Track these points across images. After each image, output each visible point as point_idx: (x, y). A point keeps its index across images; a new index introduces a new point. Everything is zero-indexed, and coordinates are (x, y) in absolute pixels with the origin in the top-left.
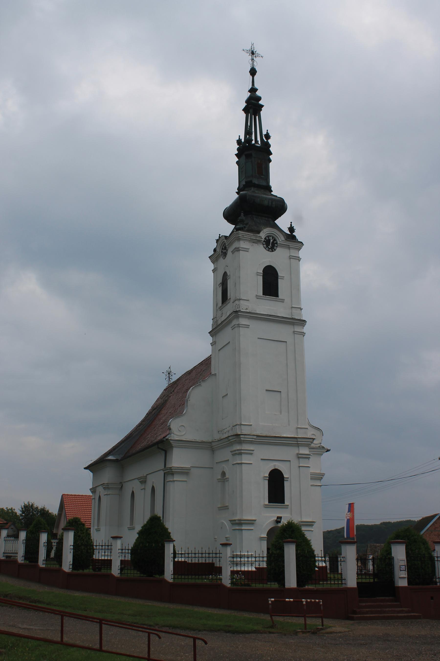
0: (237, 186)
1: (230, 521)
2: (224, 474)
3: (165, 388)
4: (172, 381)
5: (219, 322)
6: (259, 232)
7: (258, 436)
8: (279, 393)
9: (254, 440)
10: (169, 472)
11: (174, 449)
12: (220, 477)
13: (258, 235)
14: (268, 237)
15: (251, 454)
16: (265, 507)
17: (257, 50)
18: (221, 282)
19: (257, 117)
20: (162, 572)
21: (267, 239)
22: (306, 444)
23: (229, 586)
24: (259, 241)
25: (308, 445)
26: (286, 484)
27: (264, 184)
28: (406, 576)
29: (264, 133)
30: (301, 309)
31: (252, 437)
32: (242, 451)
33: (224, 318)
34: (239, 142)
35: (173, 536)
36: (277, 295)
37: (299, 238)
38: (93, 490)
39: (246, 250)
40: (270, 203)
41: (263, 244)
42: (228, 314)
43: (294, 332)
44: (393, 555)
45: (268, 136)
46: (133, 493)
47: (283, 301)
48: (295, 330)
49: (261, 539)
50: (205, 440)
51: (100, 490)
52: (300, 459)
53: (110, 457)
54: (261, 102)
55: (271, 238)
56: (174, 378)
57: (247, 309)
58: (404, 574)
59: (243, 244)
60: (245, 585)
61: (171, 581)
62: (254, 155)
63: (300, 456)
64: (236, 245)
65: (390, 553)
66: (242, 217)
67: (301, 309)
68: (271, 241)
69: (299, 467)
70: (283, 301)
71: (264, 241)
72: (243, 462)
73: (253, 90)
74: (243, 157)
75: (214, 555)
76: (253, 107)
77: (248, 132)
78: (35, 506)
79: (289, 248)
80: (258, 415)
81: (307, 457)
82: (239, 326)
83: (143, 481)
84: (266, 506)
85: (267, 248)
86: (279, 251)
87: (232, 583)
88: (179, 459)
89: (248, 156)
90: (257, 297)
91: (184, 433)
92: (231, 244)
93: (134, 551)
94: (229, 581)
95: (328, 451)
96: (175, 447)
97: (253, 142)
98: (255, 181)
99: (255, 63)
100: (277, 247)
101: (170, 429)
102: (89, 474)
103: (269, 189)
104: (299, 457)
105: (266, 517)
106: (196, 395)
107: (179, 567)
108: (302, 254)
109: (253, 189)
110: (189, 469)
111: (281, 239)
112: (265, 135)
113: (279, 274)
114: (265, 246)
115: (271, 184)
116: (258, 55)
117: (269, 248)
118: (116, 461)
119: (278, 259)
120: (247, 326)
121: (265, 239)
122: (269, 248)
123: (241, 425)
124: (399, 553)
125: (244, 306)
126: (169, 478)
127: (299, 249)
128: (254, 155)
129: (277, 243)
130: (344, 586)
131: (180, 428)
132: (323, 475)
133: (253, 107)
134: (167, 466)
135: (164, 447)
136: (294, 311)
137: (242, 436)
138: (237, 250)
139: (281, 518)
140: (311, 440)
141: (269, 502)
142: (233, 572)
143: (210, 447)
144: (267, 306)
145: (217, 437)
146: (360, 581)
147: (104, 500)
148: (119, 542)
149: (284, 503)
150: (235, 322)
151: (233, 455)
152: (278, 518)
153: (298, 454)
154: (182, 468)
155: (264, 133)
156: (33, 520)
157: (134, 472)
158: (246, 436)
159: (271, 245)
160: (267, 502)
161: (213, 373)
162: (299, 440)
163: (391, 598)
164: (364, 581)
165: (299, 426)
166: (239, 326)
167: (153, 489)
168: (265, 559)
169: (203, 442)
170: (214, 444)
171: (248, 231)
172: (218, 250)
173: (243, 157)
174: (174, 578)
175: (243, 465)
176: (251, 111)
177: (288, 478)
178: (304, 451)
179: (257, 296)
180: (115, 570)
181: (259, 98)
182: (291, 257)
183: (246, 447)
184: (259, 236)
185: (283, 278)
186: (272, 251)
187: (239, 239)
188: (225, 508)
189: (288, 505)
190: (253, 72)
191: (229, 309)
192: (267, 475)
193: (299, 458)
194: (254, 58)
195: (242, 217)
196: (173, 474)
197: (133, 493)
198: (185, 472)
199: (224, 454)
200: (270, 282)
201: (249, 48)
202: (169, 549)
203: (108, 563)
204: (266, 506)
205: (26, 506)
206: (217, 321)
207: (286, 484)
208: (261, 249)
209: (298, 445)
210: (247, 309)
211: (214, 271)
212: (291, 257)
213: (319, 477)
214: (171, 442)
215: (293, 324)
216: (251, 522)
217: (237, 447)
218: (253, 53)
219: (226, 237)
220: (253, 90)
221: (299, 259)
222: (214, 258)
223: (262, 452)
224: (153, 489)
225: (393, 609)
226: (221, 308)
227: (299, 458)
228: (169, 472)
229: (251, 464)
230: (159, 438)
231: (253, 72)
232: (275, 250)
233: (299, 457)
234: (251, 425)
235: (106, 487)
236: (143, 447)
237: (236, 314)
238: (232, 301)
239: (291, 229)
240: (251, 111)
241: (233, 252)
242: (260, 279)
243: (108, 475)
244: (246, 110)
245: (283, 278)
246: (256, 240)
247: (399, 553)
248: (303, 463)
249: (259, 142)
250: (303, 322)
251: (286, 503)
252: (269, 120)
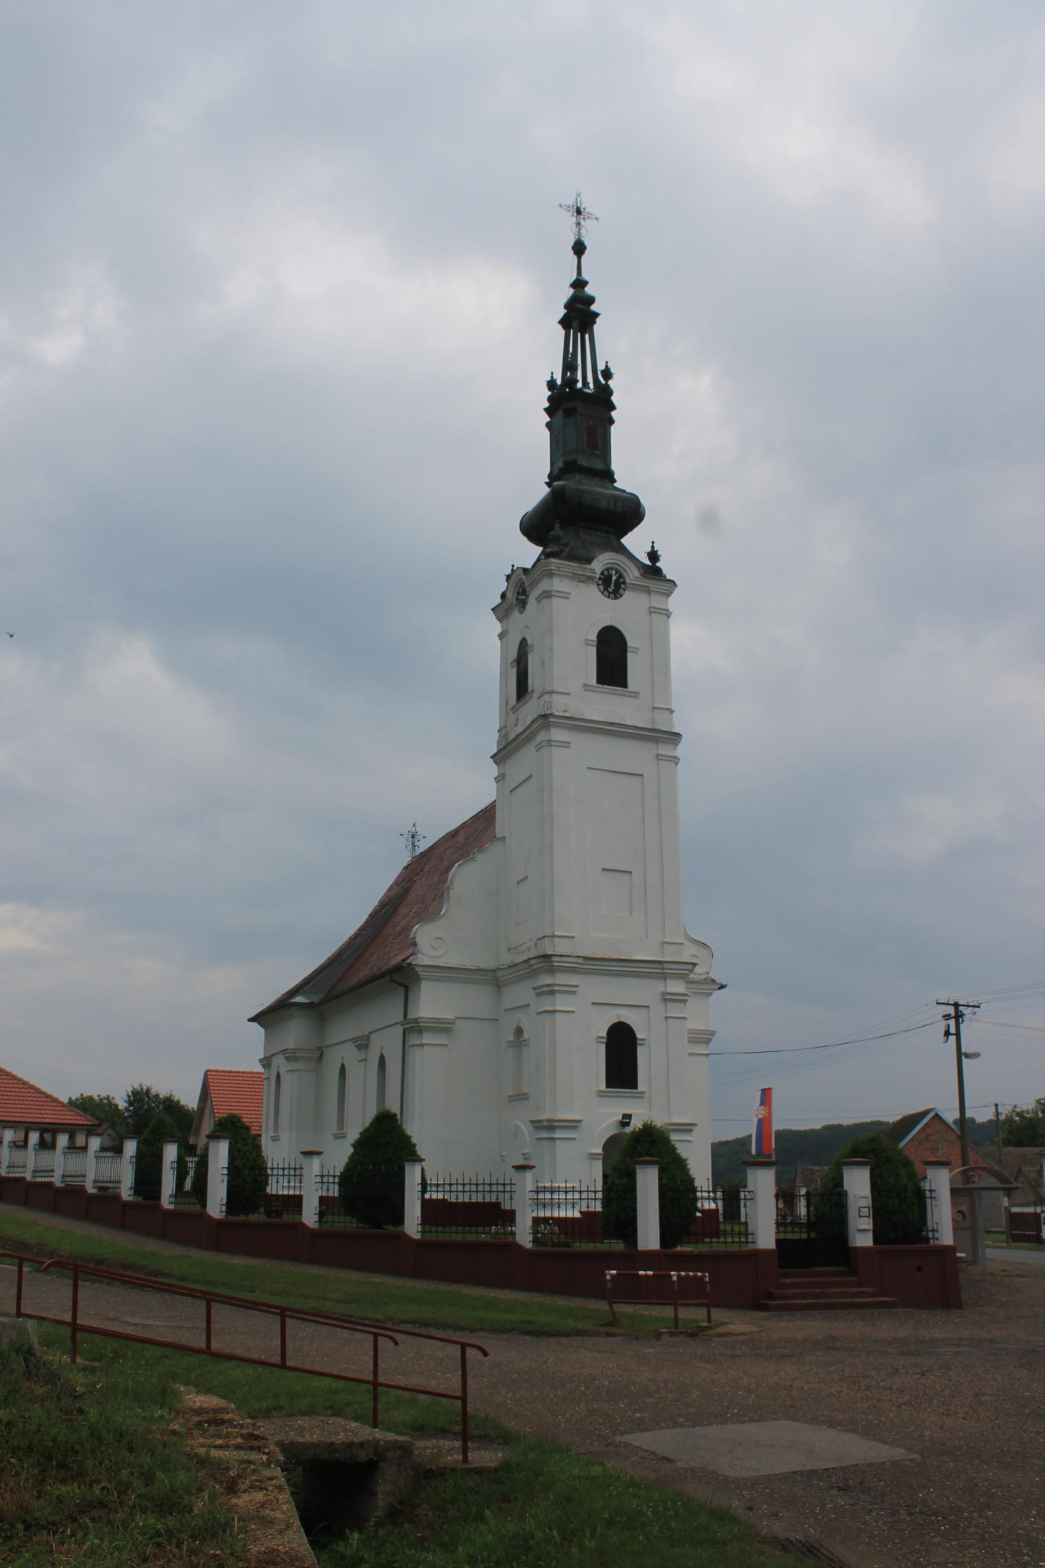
0: (547, 470)
1: (532, 1122)
2: (519, 1031)
3: (405, 864)
4: (419, 851)
5: (512, 736)
6: (589, 561)
7: (585, 958)
8: (626, 876)
10: (412, 1028)
11: (423, 983)
12: (511, 1038)
13: (588, 566)
14: (608, 570)
15: (573, 993)
17: (587, 205)
18: (515, 657)
19: (587, 336)
20: (400, 1220)
21: (606, 573)
22: (678, 974)
23: (529, 1245)
24: (590, 579)
25: (682, 977)
26: (641, 1051)
27: (599, 466)
28: (871, 1227)
29: (601, 367)
30: (672, 712)
31: (574, 960)
32: (556, 988)
33: (520, 728)
34: (551, 384)
35: (421, 1151)
36: (624, 684)
37: (668, 573)
38: (266, 1062)
39: (565, 596)
40: (612, 505)
41: (598, 585)
42: (529, 721)
43: (657, 755)
44: (846, 1187)
45: (607, 374)
46: (343, 1069)
47: (635, 695)
48: (660, 752)
49: (592, 1156)
50: (483, 965)
51: (279, 1061)
52: (669, 1004)
53: (299, 999)
54: (594, 308)
55: (614, 572)
56: (423, 846)
57: (565, 711)
58: (867, 1224)
59: (558, 584)
60: (560, 1244)
61: (417, 1236)
62: (580, 411)
63: (668, 997)
64: (544, 585)
65: (840, 1184)
66: (557, 531)
67: (672, 712)
68: (614, 578)
69: (667, 1018)
70: (635, 695)
71: (600, 579)
72: (558, 1008)
73: (579, 284)
74: (560, 415)
75: (501, 1188)
76: (579, 316)
77: (569, 365)
78: (153, 1092)
79: (648, 591)
80: (587, 918)
81: (681, 999)
82: (550, 743)
83: (363, 1044)
84: (601, 1094)
85: (606, 593)
86: (628, 597)
87: (535, 1241)
88: (431, 1002)
89: (570, 413)
90: (587, 687)
91: (442, 952)
92: (535, 584)
93: (345, 1179)
94: (530, 1238)
95: (722, 987)
96: (425, 979)
97: (579, 385)
98: (584, 462)
99: (583, 231)
101: (415, 944)
102: (258, 1031)
103: (608, 476)
104: (667, 998)
105: (602, 1115)
106: (466, 879)
107: (433, 1211)
108: (673, 602)
109: (578, 477)
110: (452, 1022)
111: (632, 574)
112: (602, 372)
113: (629, 644)
114: (602, 587)
115: (615, 466)
116: (590, 216)
117: (609, 593)
118: (310, 1006)
119: (626, 613)
120: (566, 745)
121: (602, 573)
122: (609, 593)
123: (553, 936)
124: (858, 1184)
125: (559, 706)
126: (413, 1040)
127: (668, 594)
128: (580, 411)
129: (624, 583)
130: (750, 1246)
131: (433, 943)
132: (712, 1034)
133: (579, 316)
134: (409, 1016)
135: (403, 978)
136: (658, 714)
137: (554, 959)
138: (547, 595)
139: (629, 1116)
140: (690, 967)
141: (608, 1086)
142: (537, 1221)
143: (494, 979)
144: (606, 705)
145: (506, 959)
146: (782, 1236)
147: (286, 1080)
148: (316, 1162)
149: (635, 1087)
150: (542, 736)
151: (538, 995)
152: (624, 1116)
153: (664, 994)
154: (438, 1020)
155: (601, 367)
156: (150, 1120)
157: (345, 1028)
158: (563, 959)
159: (612, 585)
160: (603, 1086)
161: (499, 835)
162: (665, 966)
163: (840, 1269)
164: (789, 1236)
165: (666, 940)
166: (550, 743)
167: (382, 1060)
168: (600, 1195)
169: (479, 970)
170: (500, 973)
171: (571, 558)
172: (509, 595)
173: (560, 415)
174: (423, 1232)
175: (557, 1014)
176: (575, 324)
177: (644, 1040)
178: (676, 987)
179: (585, 685)
180: (310, 1216)
181: (591, 300)
182: (652, 611)
183: (562, 979)
185: (636, 650)
186: (616, 598)
187: (550, 574)
188: (522, 1097)
189: (644, 1093)
190: (579, 248)
191: (530, 710)
192: (604, 1034)
193: (665, 1000)
194: (582, 222)
195: (557, 531)
196: (420, 1031)
197: (343, 1069)
198: (444, 1027)
199: (521, 993)
200: (612, 659)
201: (570, 201)
202: (413, 1176)
203: (295, 1203)
204: (601, 1094)
205: (135, 1093)
206: (506, 735)
207: (641, 1052)
208: (593, 593)
209: (664, 977)
210: (565, 711)
211: (502, 636)
212: (652, 611)
213: (704, 1038)
214: (417, 969)
215: (656, 740)
216: (573, 1125)
217: (546, 980)
218: (579, 212)
219: (525, 571)
220: (579, 284)
221: (668, 614)
222: (501, 612)
223: (592, 988)
224: (382, 1060)
225: (845, 1290)
226: (514, 710)
227: (665, 1000)
228: (412, 1028)
229: (573, 1012)
230: (393, 962)
231: (579, 248)
232: (621, 596)
233: (667, 998)
234: (573, 937)
235: (291, 1056)
236: (363, 977)
237: (545, 720)
238: (536, 695)
239: (653, 556)
240: (575, 324)
241: (539, 599)
242: (592, 653)
243: (296, 1033)
244: (565, 322)
245: (636, 650)
247: (858, 1184)
248: (674, 1010)
249: (591, 386)
250: (674, 738)
251: (641, 1086)
252: (611, 342)
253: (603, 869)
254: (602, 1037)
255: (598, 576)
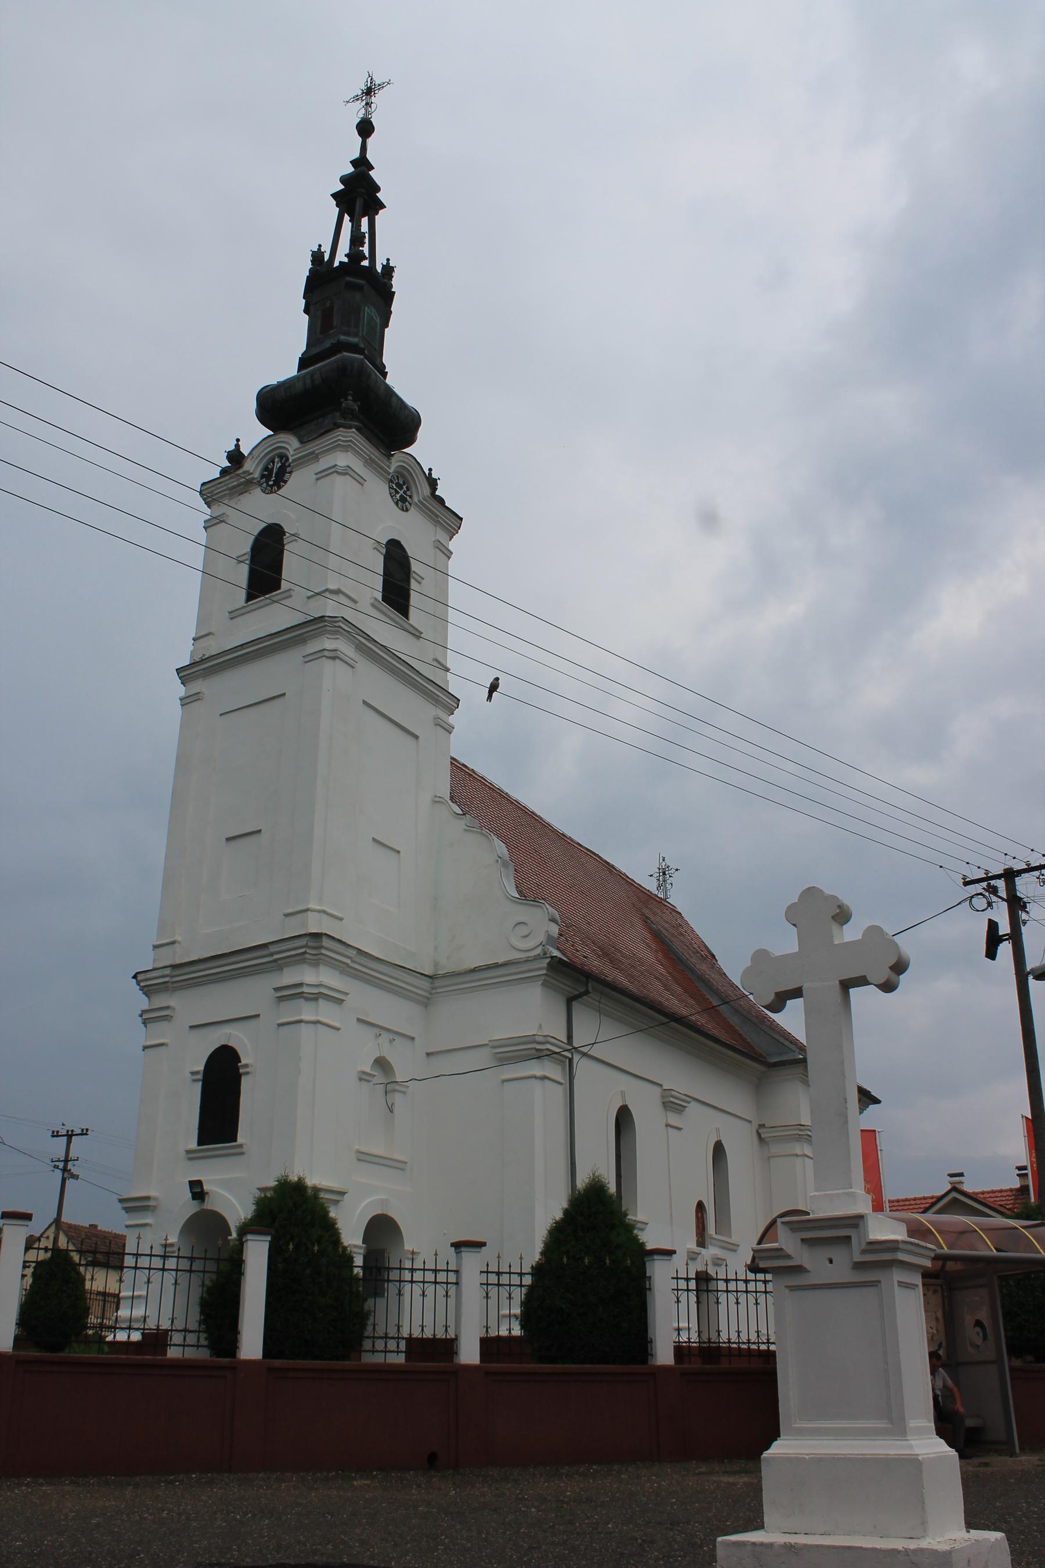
7: (174, 967)
9: (167, 979)
13: (240, 471)
16: (190, 1159)
24: (247, 485)
62: (348, 296)
73: (362, 164)
90: (234, 615)
100: (290, 473)
117: (271, 486)
121: (266, 469)
141: (200, 1143)
160: (193, 1144)
184: (244, 473)
190: (365, 128)
192: (201, 1068)
209: (278, 966)
215: (301, 640)
220: (362, 164)
231: (365, 128)
232: (285, 482)
246: (242, 484)
251: (241, 1139)
253: (228, 839)
254: (197, 1073)
255: (257, 475)
